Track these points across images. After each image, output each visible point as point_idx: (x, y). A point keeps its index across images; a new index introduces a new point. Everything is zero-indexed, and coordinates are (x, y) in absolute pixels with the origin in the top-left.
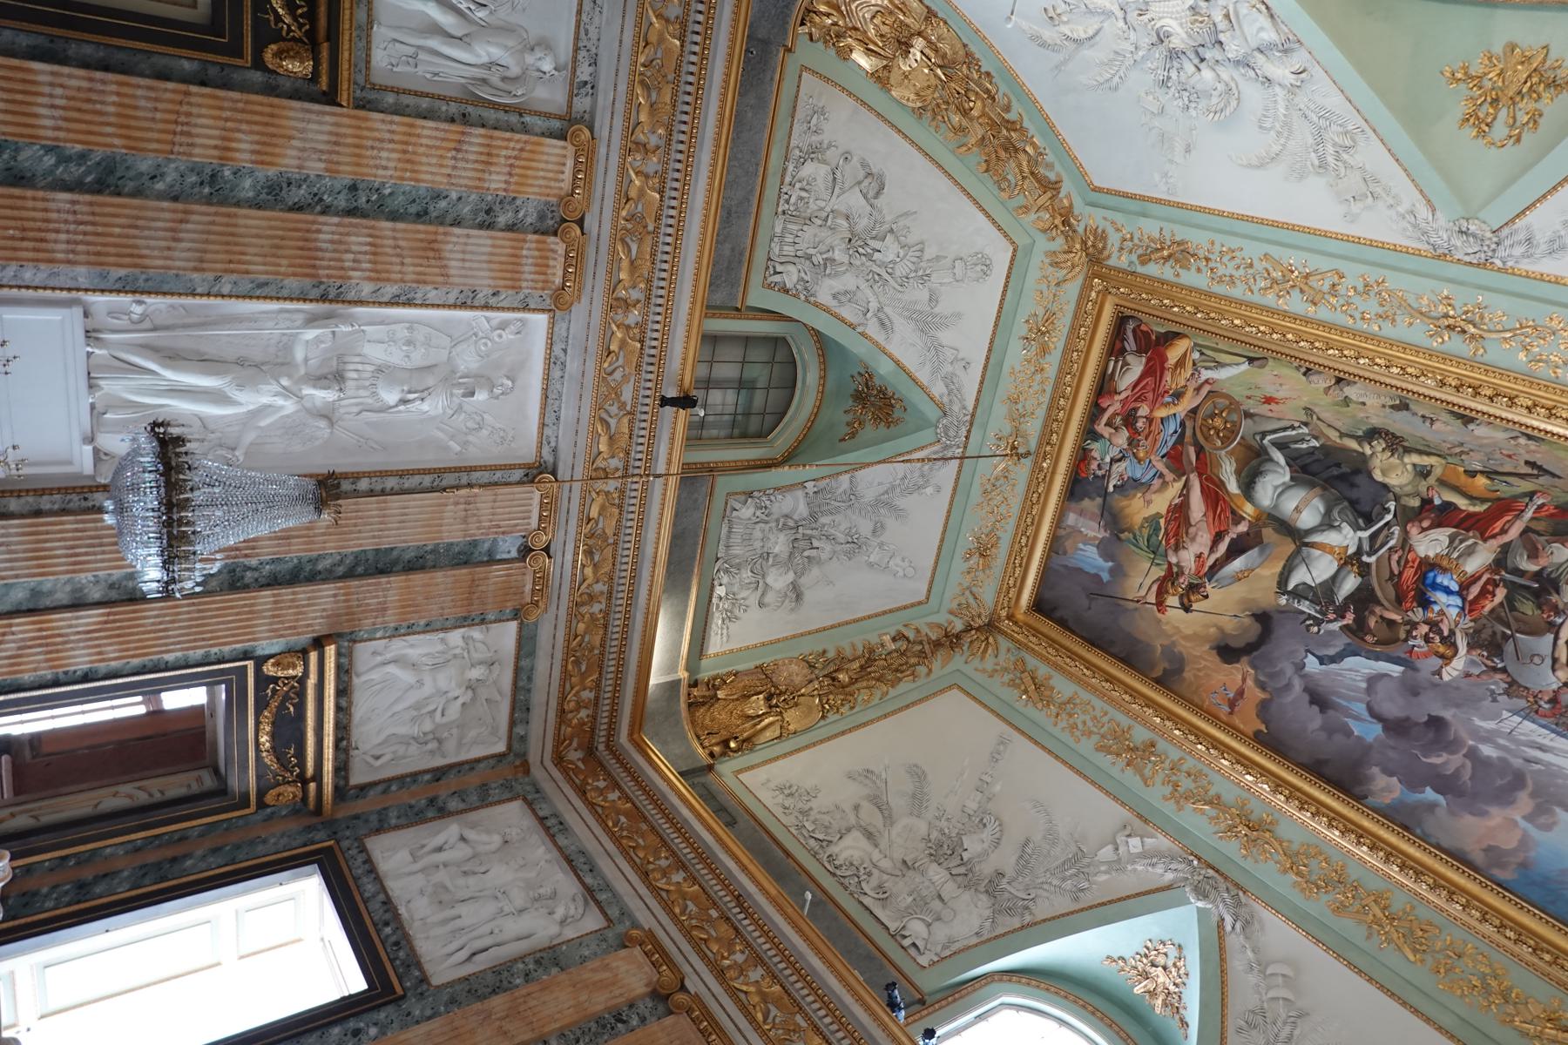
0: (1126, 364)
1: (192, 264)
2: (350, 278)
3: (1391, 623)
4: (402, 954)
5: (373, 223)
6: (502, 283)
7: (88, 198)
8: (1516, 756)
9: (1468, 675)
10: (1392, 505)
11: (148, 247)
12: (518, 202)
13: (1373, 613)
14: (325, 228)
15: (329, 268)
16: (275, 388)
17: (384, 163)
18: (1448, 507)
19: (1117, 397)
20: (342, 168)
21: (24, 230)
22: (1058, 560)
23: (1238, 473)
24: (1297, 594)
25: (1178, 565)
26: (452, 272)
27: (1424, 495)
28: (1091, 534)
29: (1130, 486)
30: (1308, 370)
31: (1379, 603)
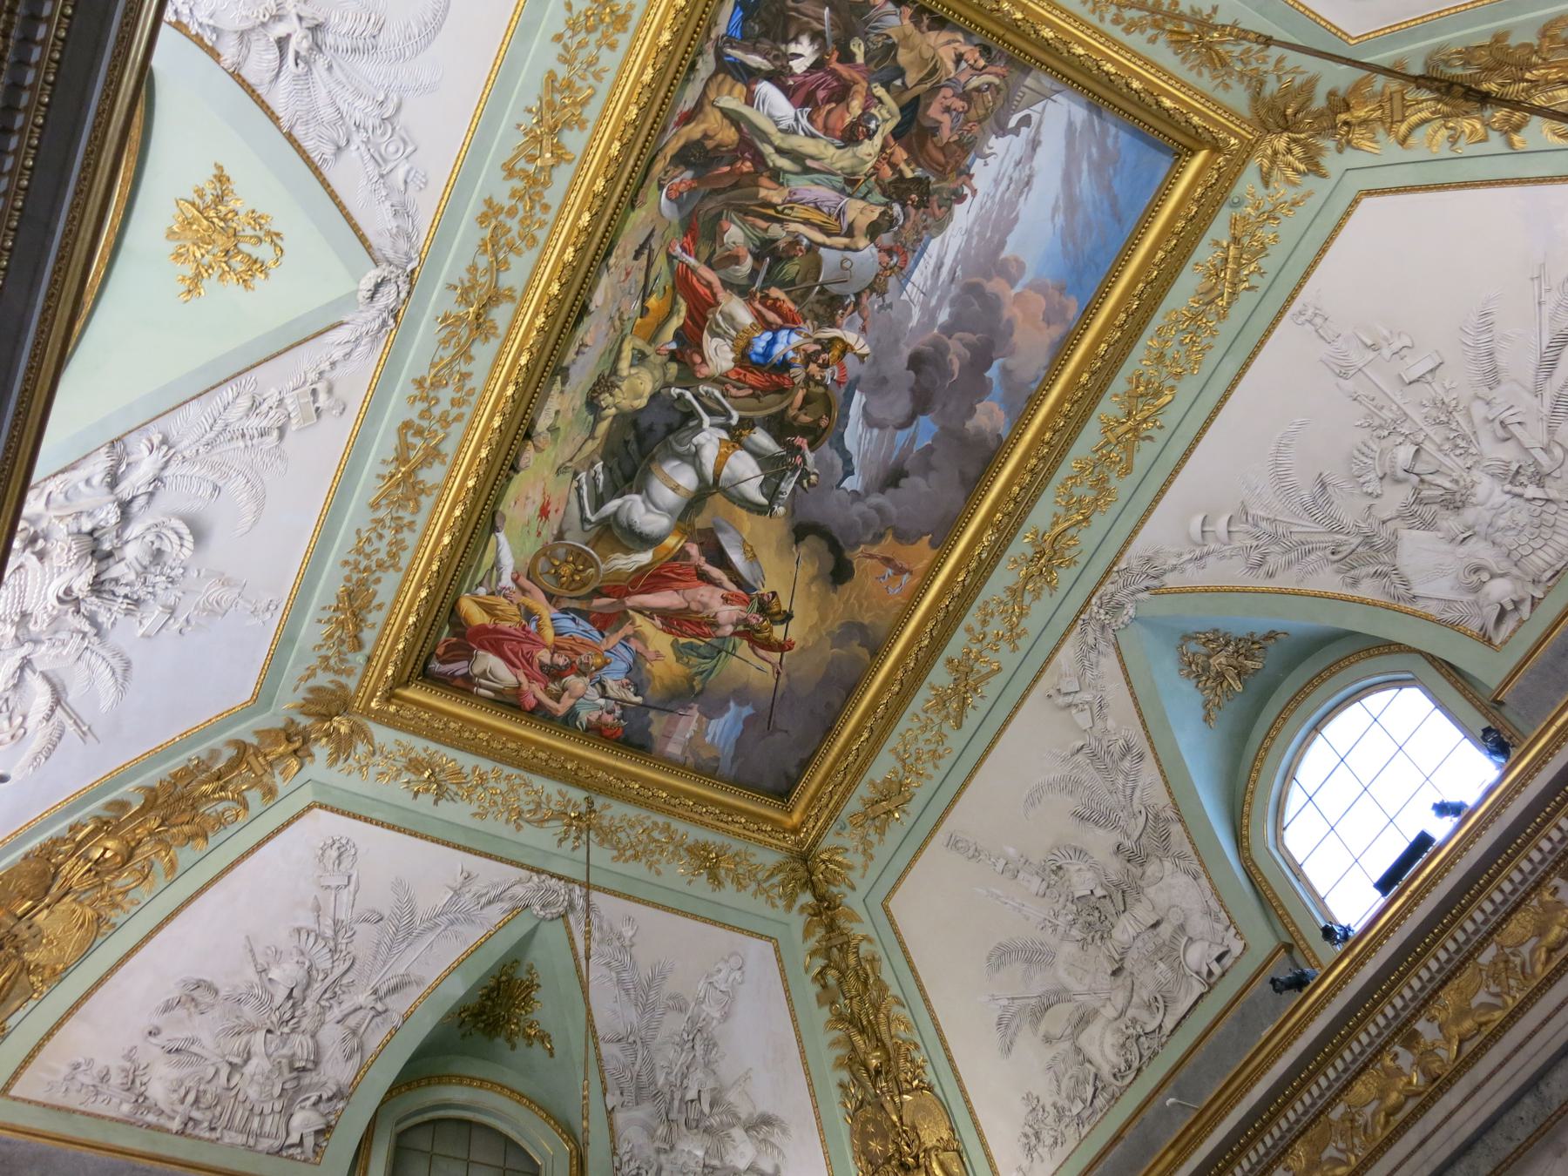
0: (483, 675)
3: (807, 400)
9: (864, 329)
10: (675, 391)
13: (795, 418)
22: (726, 767)
23: (628, 551)
24: (772, 493)
25: (736, 625)
27: (665, 359)
28: (694, 726)
29: (636, 677)
31: (784, 411)
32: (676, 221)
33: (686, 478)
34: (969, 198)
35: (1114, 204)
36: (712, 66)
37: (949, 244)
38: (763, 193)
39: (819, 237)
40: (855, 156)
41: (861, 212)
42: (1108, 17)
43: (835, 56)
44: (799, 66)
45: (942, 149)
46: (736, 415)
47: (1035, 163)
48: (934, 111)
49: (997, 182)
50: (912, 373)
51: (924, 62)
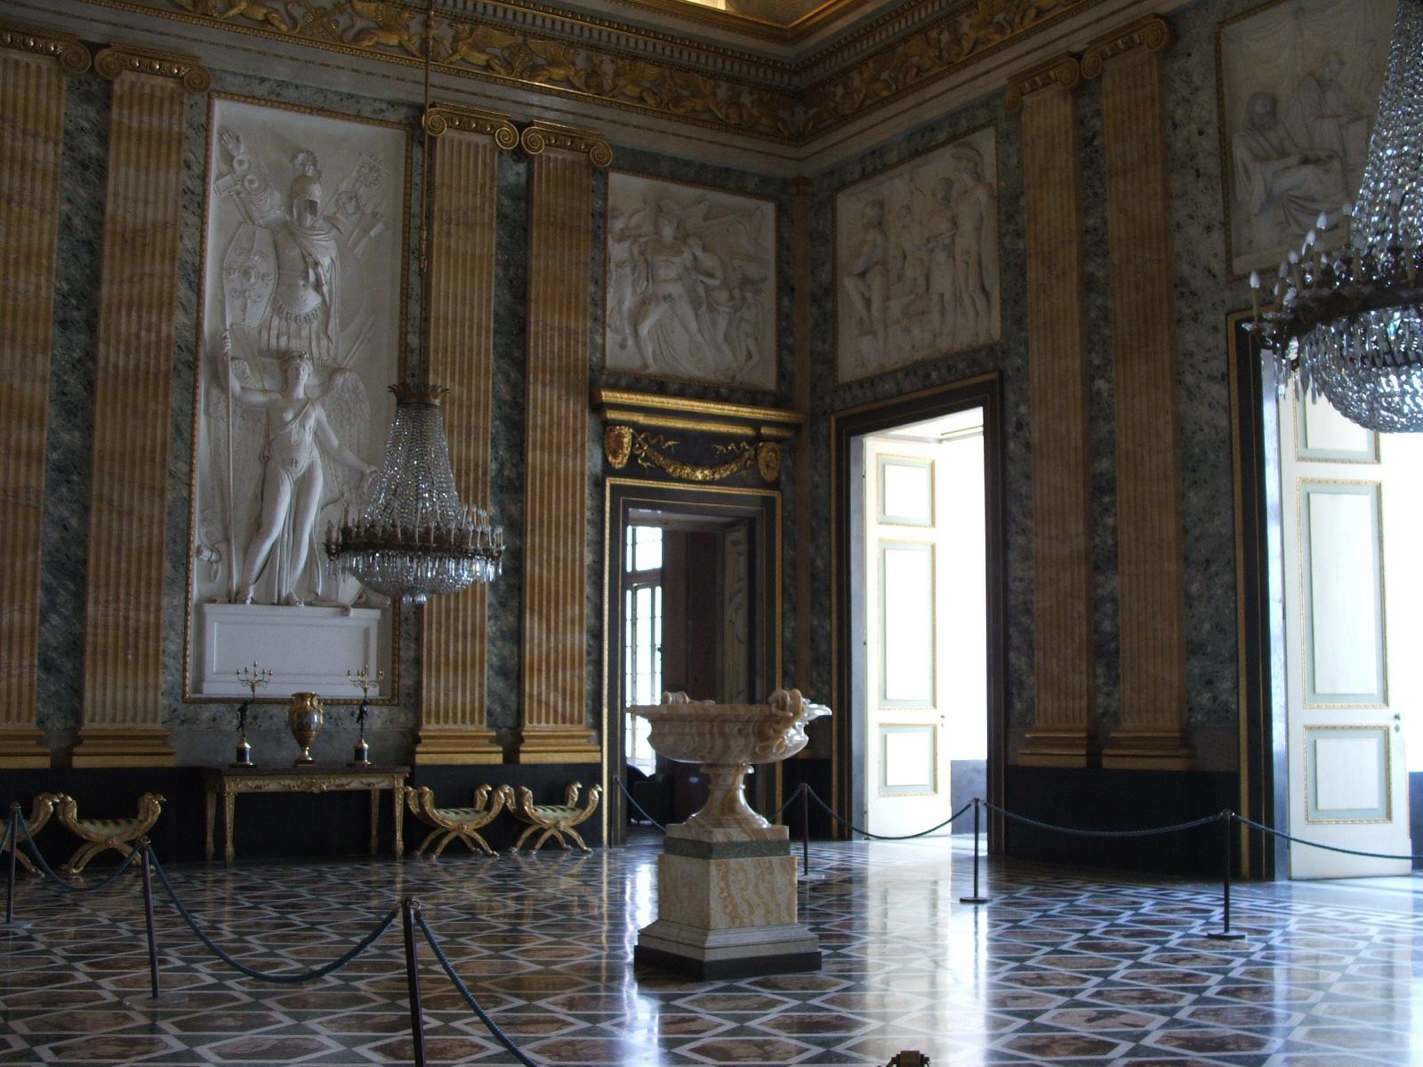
1: (157, 499)
2: (169, 336)
4: (961, 366)
5: (104, 306)
6: (174, 158)
7: (91, 588)
11: (140, 538)
12: (71, 127)
14: (112, 359)
15: (157, 359)
16: (295, 427)
17: (32, 289)
20: (41, 336)
21: (127, 646)
26: (160, 217)
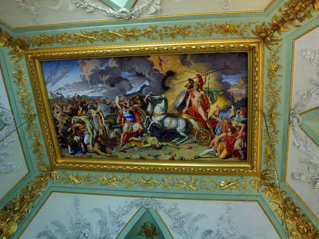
3: (135, 103)
8: (95, 87)
9: (114, 100)
10: (149, 132)
13: (140, 104)
18: (137, 137)
19: (240, 136)
22: (243, 75)
23: (192, 125)
24: (160, 100)
25: (199, 91)
27: (143, 137)
28: (234, 89)
30: (182, 159)
32: (116, 147)
33: (167, 121)
34: (77, 94)
35: (57, 66)
36: (87, 153)
37: (87, 93)
38: (102, 133)
39: (103, 119)
40: (85, 120)
41: (94, 113)
42: (30, 96)
43: (73, 133)
44: (79, 138)
45: (73, 105)
46: (147, 117)
47: (63, 86)
48: (68, 111)
49: (71, 91)
50: (115, 85)
51: (63, 118)
